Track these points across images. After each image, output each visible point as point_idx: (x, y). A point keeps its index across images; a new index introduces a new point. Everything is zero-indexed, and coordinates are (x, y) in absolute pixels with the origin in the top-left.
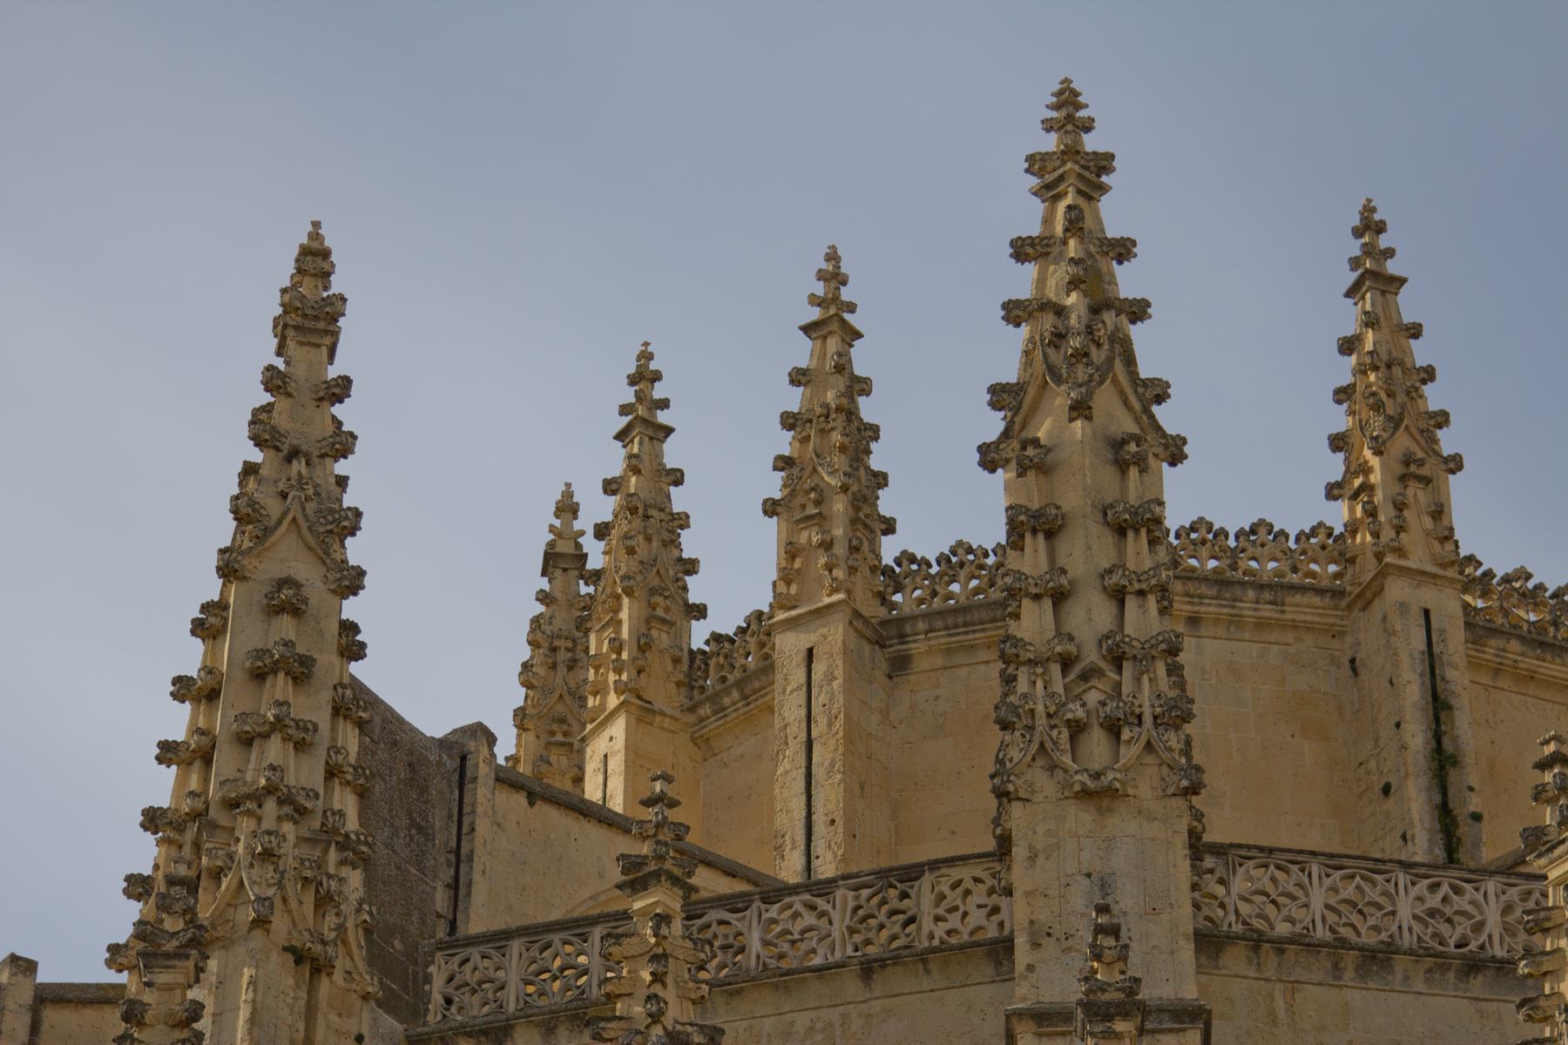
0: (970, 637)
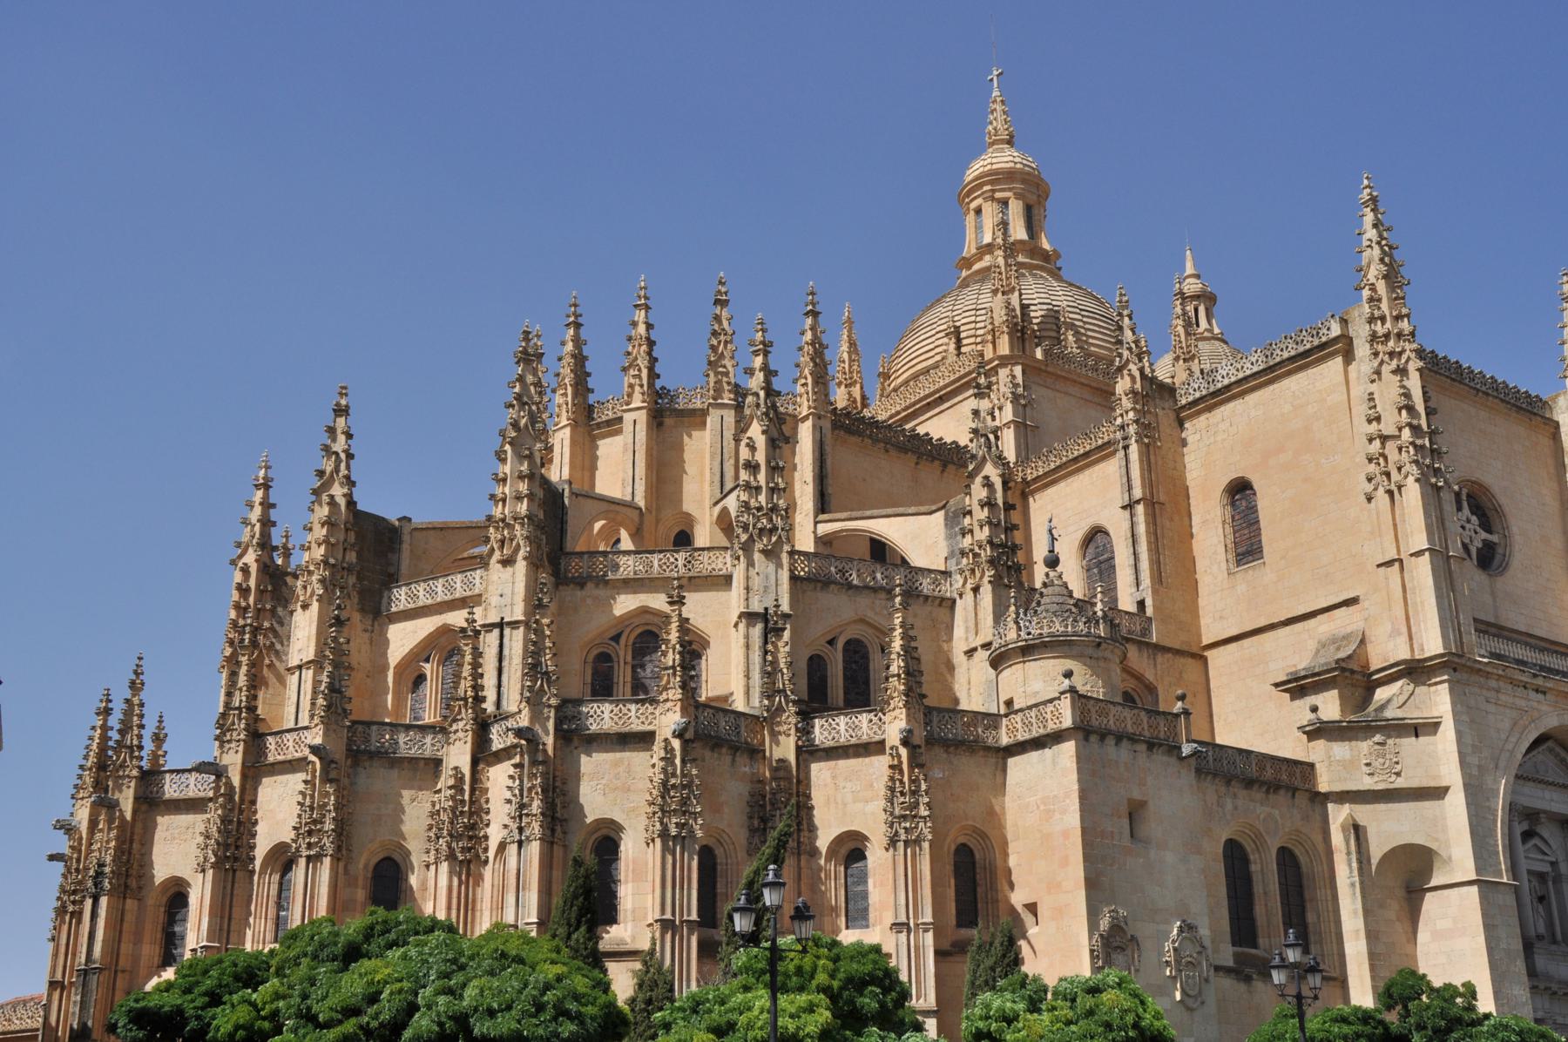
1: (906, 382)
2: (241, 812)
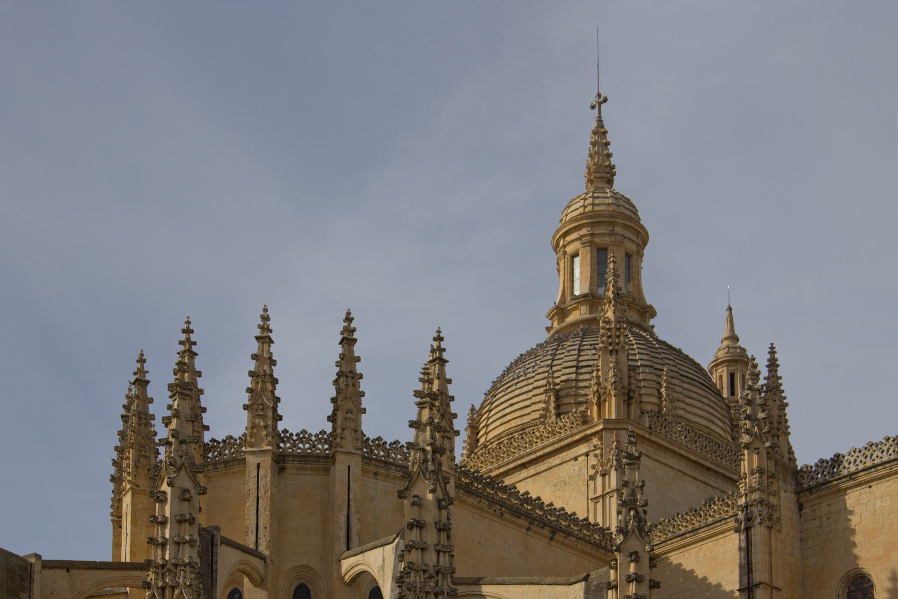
0: (306, 465)
1: (499, 437)
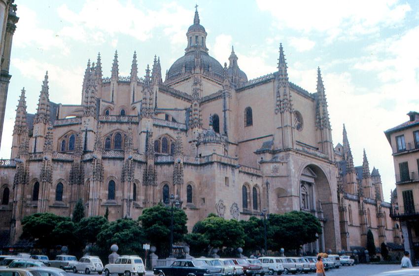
2: (26, 170)
